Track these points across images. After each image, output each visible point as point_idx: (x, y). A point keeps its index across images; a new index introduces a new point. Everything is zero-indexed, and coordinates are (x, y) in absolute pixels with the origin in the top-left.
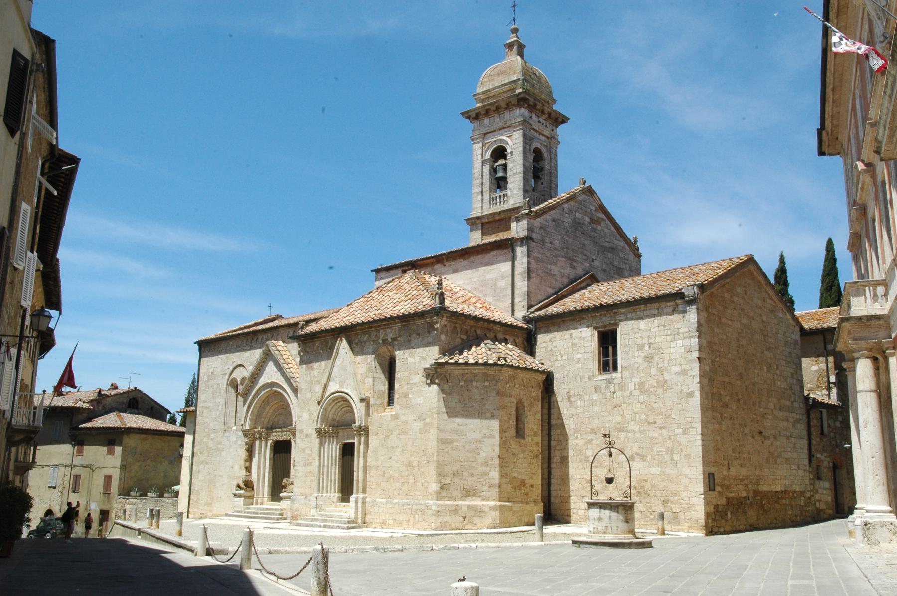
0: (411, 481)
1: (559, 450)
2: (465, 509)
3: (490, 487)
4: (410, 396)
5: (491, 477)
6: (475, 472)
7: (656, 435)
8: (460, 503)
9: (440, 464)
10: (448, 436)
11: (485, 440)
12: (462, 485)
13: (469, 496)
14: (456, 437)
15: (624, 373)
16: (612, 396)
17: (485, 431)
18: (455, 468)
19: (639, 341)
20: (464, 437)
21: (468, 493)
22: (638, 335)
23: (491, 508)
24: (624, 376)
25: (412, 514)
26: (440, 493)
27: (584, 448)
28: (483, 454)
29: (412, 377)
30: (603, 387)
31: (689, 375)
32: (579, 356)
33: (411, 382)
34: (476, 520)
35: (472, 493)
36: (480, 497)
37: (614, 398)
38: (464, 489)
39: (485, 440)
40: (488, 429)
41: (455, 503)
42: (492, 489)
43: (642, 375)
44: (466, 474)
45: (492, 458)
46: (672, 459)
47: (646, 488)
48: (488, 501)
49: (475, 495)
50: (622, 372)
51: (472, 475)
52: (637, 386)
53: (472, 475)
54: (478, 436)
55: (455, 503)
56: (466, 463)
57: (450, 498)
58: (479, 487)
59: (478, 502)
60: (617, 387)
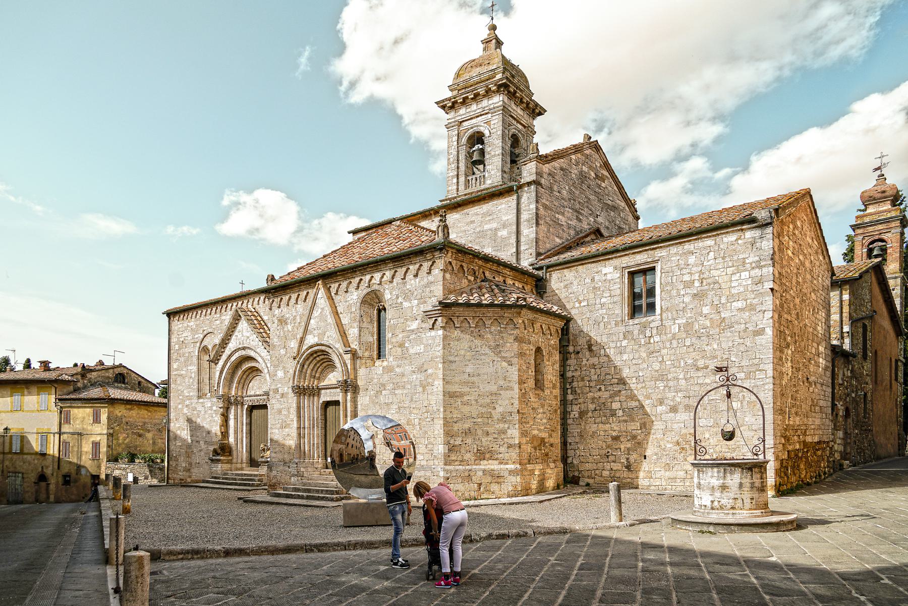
1: (576, 404)
2: (480, 473)
3: (508, 447)
4: (407, 345)
5: (509, 436)
6: (491, 430)
8: (474, 467)
9: (447, 422)
11: (501, 392)
12: (475, 446)
13: (484, 459)
14: (466, 389)
15: (664, 315)
16: (648, 341)
17: (501, 382)
18: (466, 426)
19: (687, 278)
20: (476, 389)
21: (481, 455)
22: (684, 271)
23: (511, 472)
24: (664, 318)
26: (449, 456)
27: (610, 400)
28: (499, 409)
29: (408, 323)
30: (636, 332)
31: (758, 310)
32: (603, 300)
33: (408, 329)
34: (495, 487)
35: (487, 456)
37: (650, 343)
38: (478, 450)
39: (501, 392)
43: (689, 315)
44: (479, 432)
48: (507, 464)
49: (491, 458)
50: (661, 315)
51: (488, 434)
52: (682, 328)
53: (488, 434)
54: (494, 388)
56: (479, 420)
57: (461, 461)
58: (496, 447)
59: (493, 465)
60: (654, 331)
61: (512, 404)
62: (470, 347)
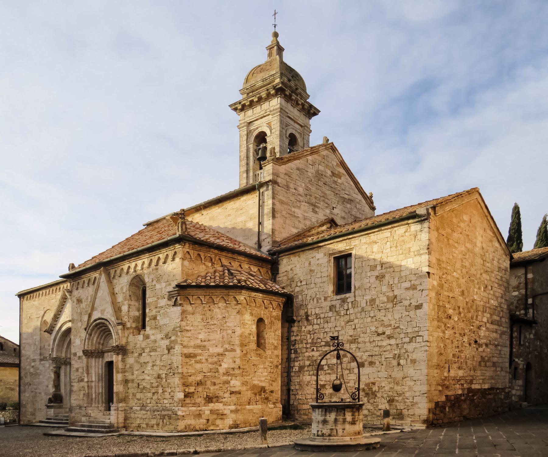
0: (160, 391)
2: (207, 412)
3: (231, 394)
6: (217, 381)
7: (384, 343)
10: (191, 350)
12: (205, 393)
17: (227, 346)
23: (232, 411)
25: (161, 419)
28: (225, 366)
36: (221, 402)
38: (207, 396)
39: (226, 353)
40: (230, 344)
41: (199, 408)
42: (233, 395)
44: (209, 383)
45: (233, 369)
46: (399, 364)
47: (374, 389)
48: (230, 405)
49: (217, 401)
51: (215, 384)
54: (220, 350)
55: (199, 408)
56: (209, 374)
57: (194, 404)
58: (221, 394)
61: (235, 362)
62: (202, 319)
